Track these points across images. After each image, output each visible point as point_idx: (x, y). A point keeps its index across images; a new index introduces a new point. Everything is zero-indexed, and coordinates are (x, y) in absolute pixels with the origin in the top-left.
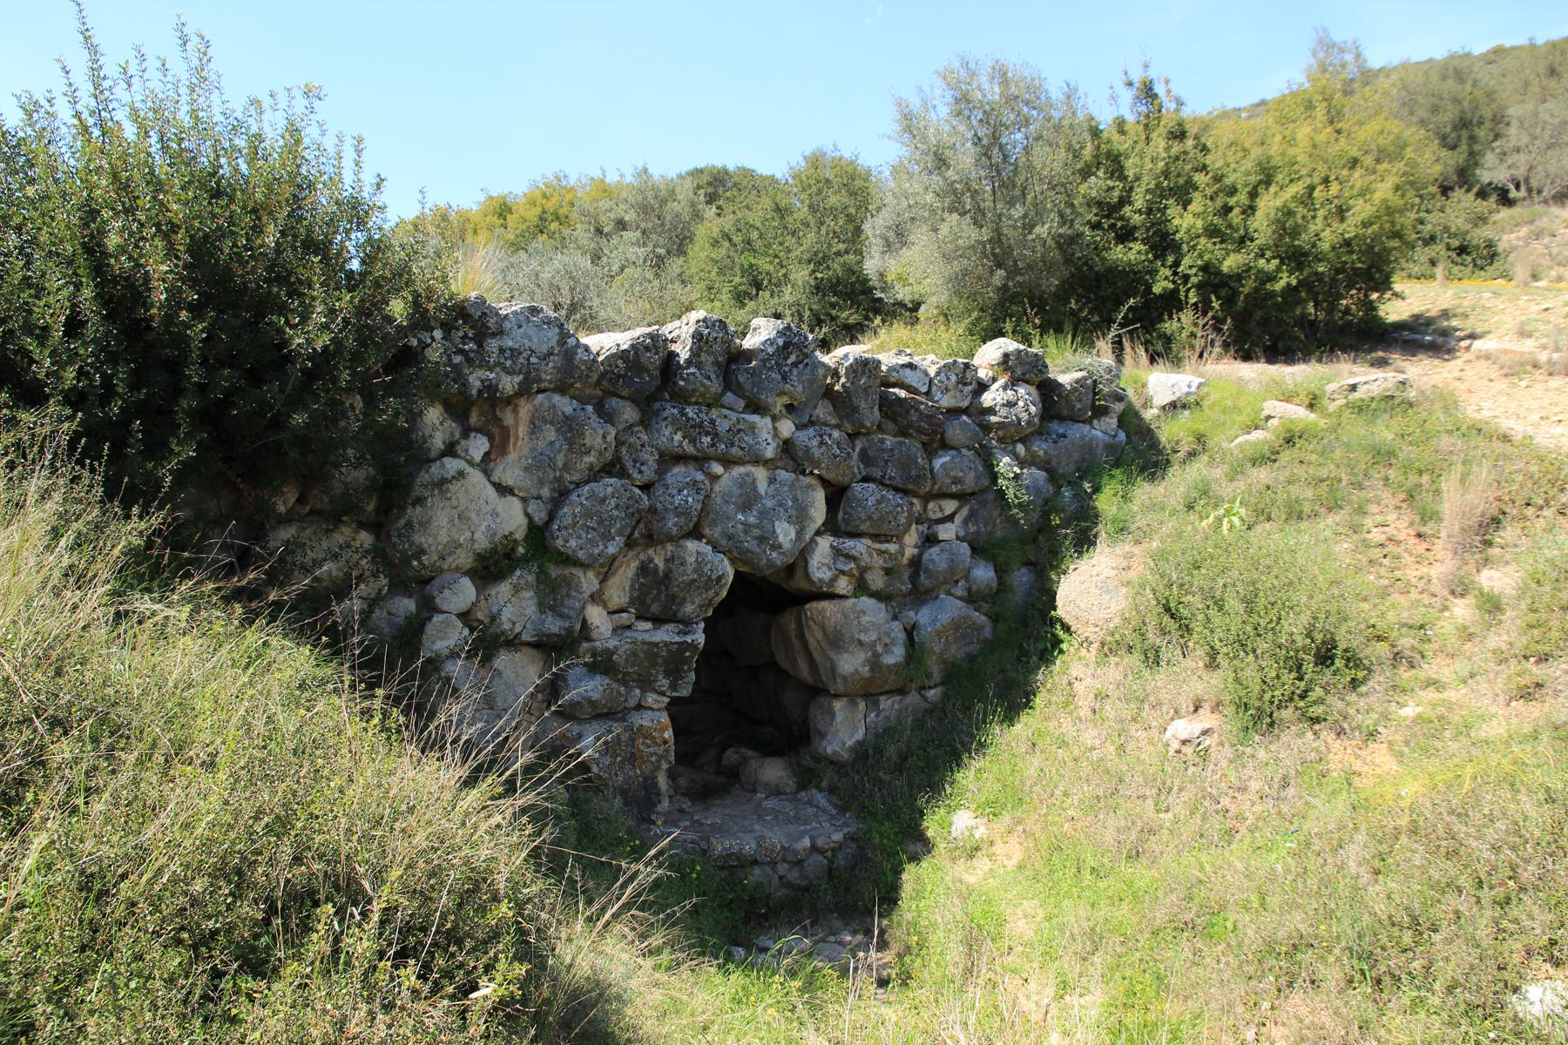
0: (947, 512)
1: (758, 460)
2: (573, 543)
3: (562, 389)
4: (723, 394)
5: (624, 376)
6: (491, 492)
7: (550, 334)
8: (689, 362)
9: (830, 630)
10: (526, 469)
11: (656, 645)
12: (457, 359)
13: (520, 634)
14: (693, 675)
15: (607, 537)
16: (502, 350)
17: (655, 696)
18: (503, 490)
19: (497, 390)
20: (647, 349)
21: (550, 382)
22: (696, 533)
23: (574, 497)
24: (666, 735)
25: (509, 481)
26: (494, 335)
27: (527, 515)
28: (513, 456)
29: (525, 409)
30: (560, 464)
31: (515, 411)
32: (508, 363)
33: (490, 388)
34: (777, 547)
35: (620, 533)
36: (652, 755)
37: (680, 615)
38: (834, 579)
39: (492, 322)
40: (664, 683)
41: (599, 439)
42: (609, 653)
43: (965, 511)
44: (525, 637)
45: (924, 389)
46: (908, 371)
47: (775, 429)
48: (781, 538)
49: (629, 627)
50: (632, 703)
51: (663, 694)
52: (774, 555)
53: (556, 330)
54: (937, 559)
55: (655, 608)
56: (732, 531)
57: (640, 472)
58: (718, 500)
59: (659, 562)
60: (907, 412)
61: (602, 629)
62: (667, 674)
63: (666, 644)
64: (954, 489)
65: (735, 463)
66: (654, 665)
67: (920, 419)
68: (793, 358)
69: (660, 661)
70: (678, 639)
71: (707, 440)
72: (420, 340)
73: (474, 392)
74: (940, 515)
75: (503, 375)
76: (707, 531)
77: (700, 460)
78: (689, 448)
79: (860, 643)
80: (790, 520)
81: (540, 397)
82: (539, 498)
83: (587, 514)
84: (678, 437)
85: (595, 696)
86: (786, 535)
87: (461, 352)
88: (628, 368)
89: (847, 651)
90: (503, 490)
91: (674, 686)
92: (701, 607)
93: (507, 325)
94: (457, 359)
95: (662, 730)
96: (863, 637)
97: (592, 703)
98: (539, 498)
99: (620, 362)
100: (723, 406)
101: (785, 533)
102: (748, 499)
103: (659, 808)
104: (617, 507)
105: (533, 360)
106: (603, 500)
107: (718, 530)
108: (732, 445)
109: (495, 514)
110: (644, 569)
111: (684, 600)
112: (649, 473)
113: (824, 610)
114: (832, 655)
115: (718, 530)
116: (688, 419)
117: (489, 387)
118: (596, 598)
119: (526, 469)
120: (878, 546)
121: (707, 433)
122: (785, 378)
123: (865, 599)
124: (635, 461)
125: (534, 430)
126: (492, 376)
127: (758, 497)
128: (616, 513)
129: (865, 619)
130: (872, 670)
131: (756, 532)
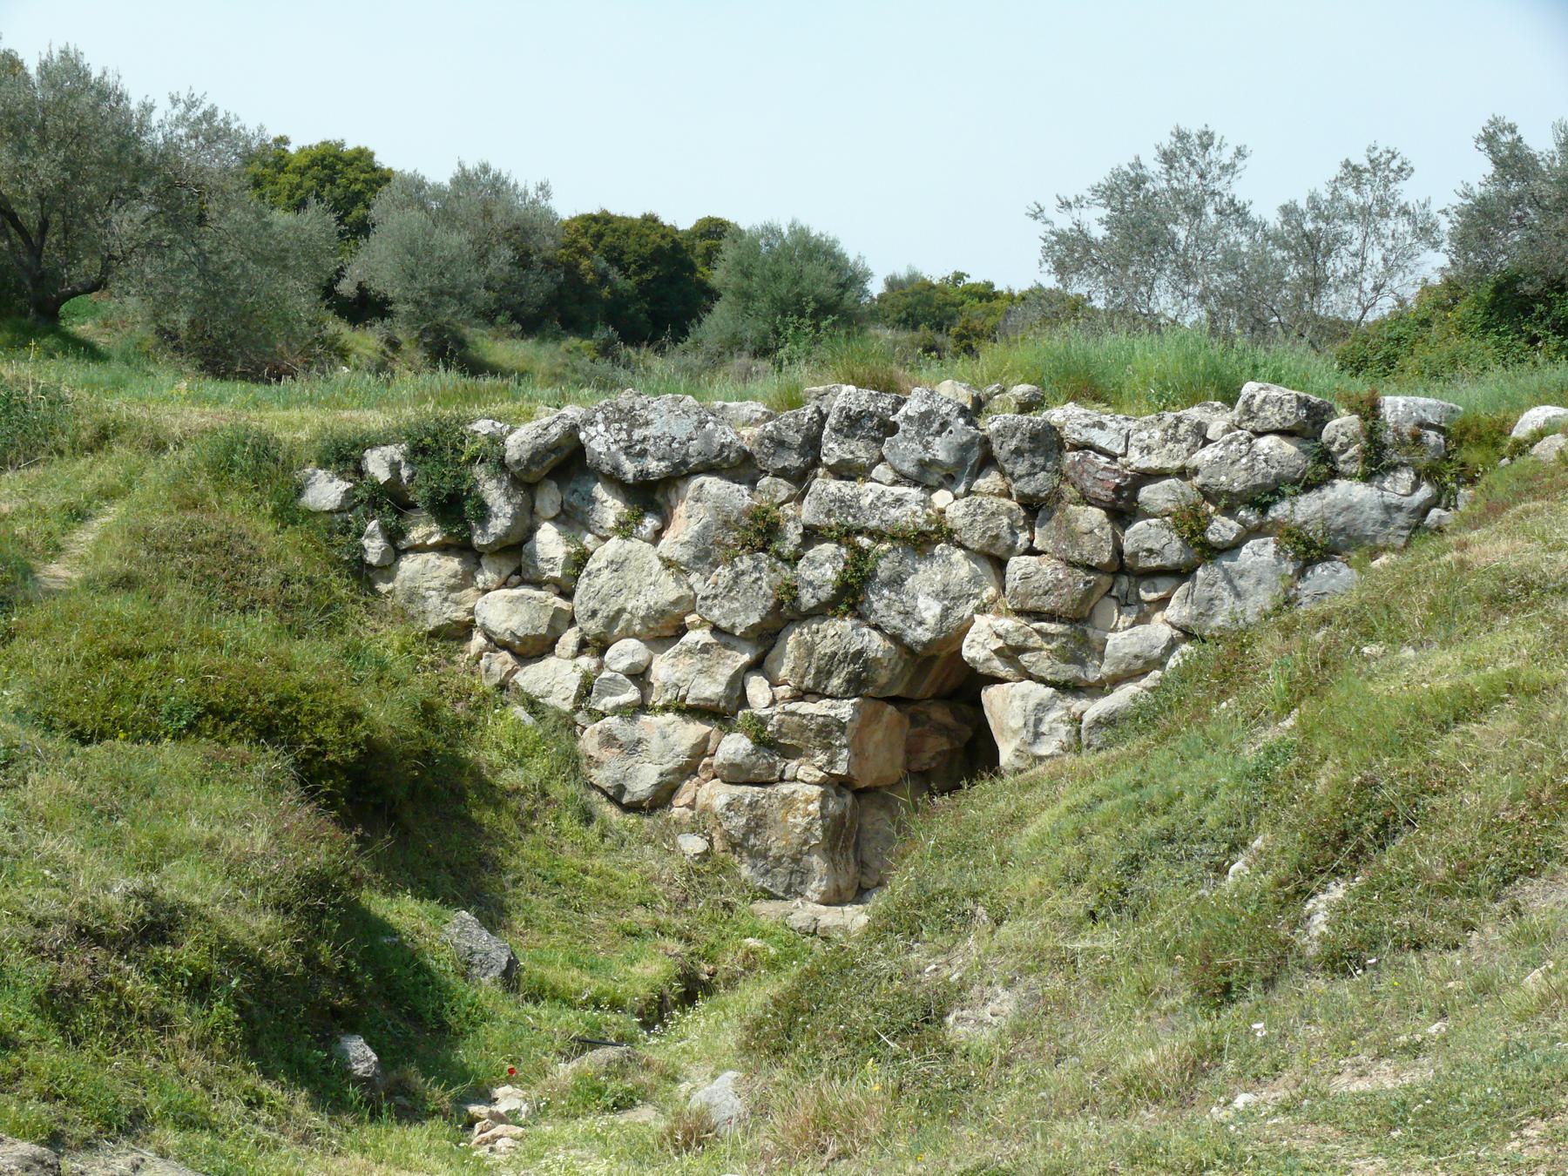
3: (709, 469)
6: (658, 565)
11: (803, 716)
12: (614, 448)
14: (845, 752)
18: (668, 563)
26: (640, 426)
33: (644, 473)
36: (795, 826)
38: (988, 660)
40: (821, 758)
42: (762, 721)
48: (924, 615)
51: (820, 769)
52: (920, 630)
55: (809, 682)
63: (813, 717)
64: (1154, 562)
73: (630, 476)
95: (808, 801)
118: (756, 666)
122: (926, 447)
123: (1027, 682)
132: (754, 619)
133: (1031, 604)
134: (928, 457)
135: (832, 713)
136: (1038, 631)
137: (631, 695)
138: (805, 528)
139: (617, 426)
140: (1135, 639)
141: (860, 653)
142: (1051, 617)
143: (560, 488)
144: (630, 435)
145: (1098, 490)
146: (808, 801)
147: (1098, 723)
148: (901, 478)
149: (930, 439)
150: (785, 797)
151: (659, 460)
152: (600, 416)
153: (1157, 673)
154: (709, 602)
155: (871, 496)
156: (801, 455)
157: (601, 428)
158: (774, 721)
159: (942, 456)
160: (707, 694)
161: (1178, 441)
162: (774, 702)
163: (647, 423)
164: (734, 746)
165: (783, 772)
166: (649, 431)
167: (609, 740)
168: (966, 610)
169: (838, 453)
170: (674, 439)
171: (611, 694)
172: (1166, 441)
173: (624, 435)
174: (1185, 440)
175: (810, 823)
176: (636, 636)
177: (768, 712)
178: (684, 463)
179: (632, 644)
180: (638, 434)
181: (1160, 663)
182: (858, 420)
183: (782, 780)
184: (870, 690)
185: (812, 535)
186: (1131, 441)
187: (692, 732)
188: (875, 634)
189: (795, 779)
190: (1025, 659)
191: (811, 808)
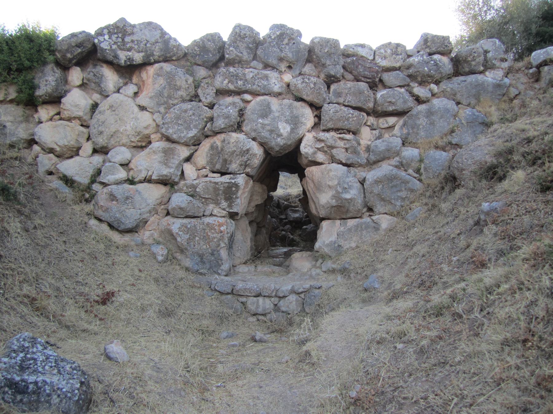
0: (390, 124)
1: (270, 94)
2: (171, 131)
4: (251, 61)
5: (199, 55)
6: (136, 109)
7: (156, 33)
8: (230, 45)
9: (316, 181)
10: (151, 98)
11: (216, 183)
13: (151, 176)
15: (188, 128)
16: (133, 41)
17: (219, 210)
18: (142, 108)
19: (133, 60)
20: (209, 40)
21: (159, 57)
22: (238, 127)
23: (172, 110)
24: (222, 228)
25: (143, 103)
26: (129, 35)
27: (154, 120)
28: (144, 93)
29: (151, 70)
30: (166, 95)
31: (147, 73)
32: (136, 47)
34: (280, 135)
35: (195, 127)
36: (214, 238)
37: (230, 170)
38: (315, 153)
39: (129, 29)
40: (224, 204)
41: (184, 83)
42: (194, 187)
43: (401, 122)
44: (154, 177)
45: (371, 58)
46: (360, 49)
47: (281, 78)
48: (282, 131)
49: (207, 176)
50: (207, 213)
51: (224, 209)
52: (279, 139)
53: (160, 31)
54: (379, 145)
55: (218, 167)
56: (255, 127)
57: (206, 98)
58: (249, 113)
59: (219, 144)
60: (357, 67)
61: (191, 175)
62: (226, 199)
64: (391, 109)
65: (259, 95)
66: (218, 195)
67: (365, 70)
68: (286, 41)
69: (221, 192)
70: (228, 181)
71: (240, 83)
72: (99, 40)
73: (123, 62)
74: (386, 126)
75: (134, 52)
76: (244, 129)
77: (238, 93)
78: (231, 87)
79: (330, 187)
80: (287, 122)
81: (157, 65)
82: (159, 112)
83: (178, 118)
84: (226, 82)
85: (183, 205)
86: (284, 129)
87: (115, 43)
88: (200, 51)
89: (324, 192)
90: (142, 108)
91: (230, 206)
92: (241, 165)
93: (135, 30)
94: (114, 47)
95: (220, 225)
96: (330, 183)
97: (181, 208)
98: (159, 112)
99: (196, 48)
100: (250, 67)
101: (285, 129)
102: (266, 112)
103: (223, 267)
104: (194, 114)
105: (148, 45)
106: (186, 111)
107: (249, 127)
108: (254, 84)
109: (136, 119)
110: (212, 147)
111: (231, 161)
112: (210, 99)
113: (312, 171)
114: (318, 195)
115: (249, 127)
116: (230, 73)
117: (129, 59)
118: (188, 159)
119: (151, 98)
120: (339, 136)
121: (241, 80)
123: (334, 165)
124: (204, 94)
125: (155, 79)
126: (130, 54)
127: (270, 111)
128: (193, 117)
129: (331, 174)
130: (337, 201)
131: (268, 128)
132: (193, 133)
133: (340, 125)
134: (283, 55)
135: (233, 181)
136: (340, 138)
137: (122, 174)
138: (217, 90)
139: (116, 36)
140: (385, 143)
141: (248, 150)
142: (349, 131)
143: (82, 70)
144: (123, 40)
145: (366, 73)
146: (220, 225)
147: (377, 182)
148: (267, 66)
149: (283, 46)
150: (208, 224)
151: (139, 52)
152: (106, 31)
153: (397, 159)
154: (166, 126)
155: (251, 75)
156: (213, 55)
157: (107, 37)
158: (200, 186)
159: (290, 55)
160: (165, 173)
161: (398, 55)
162: (198, 177)
163: (133, 33)
164: (179, 199)
165: (204, 211)
166: (135, 38)
167: (113, 197)
168: (301, 132)
169: (235, 52)
170: (148, 41)
171: (113, 174)
172: (393, 54)
173: (120, 40)
174: (401, 54)
175: (222, 236)
176: (124, 145)
177: (197, 182)
178: (153, 55)
179: (123, 149)
180: (128, 39)
181: (398, 154)
182: (244, 38)
183: (204, 215)
184: (248, 170)
185: (221, 93)
186: (377, 53)
187: (153, 194)
188: (254, 143)
189: (211, 215)
190: (334, 151)
191: (222, 228)
